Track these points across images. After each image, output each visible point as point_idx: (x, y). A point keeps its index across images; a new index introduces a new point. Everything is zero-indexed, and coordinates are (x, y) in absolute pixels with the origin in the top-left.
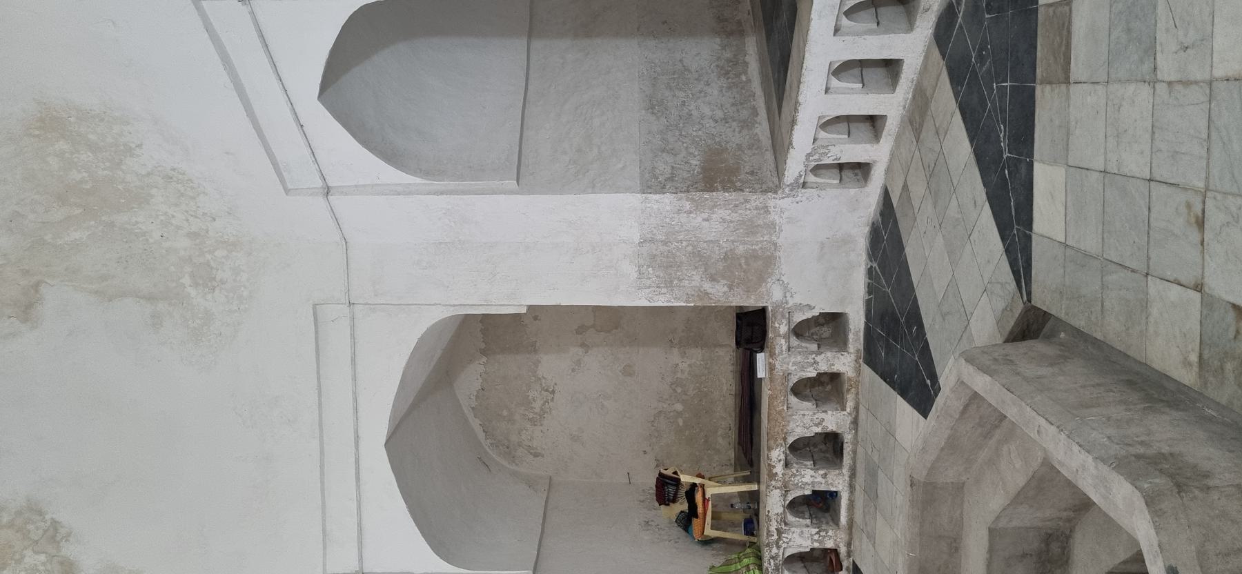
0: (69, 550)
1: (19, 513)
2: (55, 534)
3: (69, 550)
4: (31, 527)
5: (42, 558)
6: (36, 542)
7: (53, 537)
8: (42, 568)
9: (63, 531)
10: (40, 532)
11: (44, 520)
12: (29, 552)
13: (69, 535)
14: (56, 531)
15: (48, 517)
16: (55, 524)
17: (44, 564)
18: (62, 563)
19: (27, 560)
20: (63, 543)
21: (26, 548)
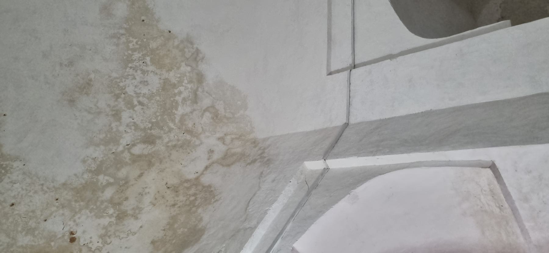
0: (202, 67)
1: (182, 42)
2: (197, 57)
3: (202, 67)
4: (186, 50)
5: (189, 69)
6: (187, 59)
7: (196, 59)
8: (188, 74)
9: (201, 56)
10: (190, 54)
11: (193, 48)
12: (183, 64)
13: (203, 58)
14: (197, 54)
15: (195, 46)
16: (198, 51)
17: (189, 72)
18: (197, 74)
19: (182, 68)
20: (200, 62)
21: (182, 61)
